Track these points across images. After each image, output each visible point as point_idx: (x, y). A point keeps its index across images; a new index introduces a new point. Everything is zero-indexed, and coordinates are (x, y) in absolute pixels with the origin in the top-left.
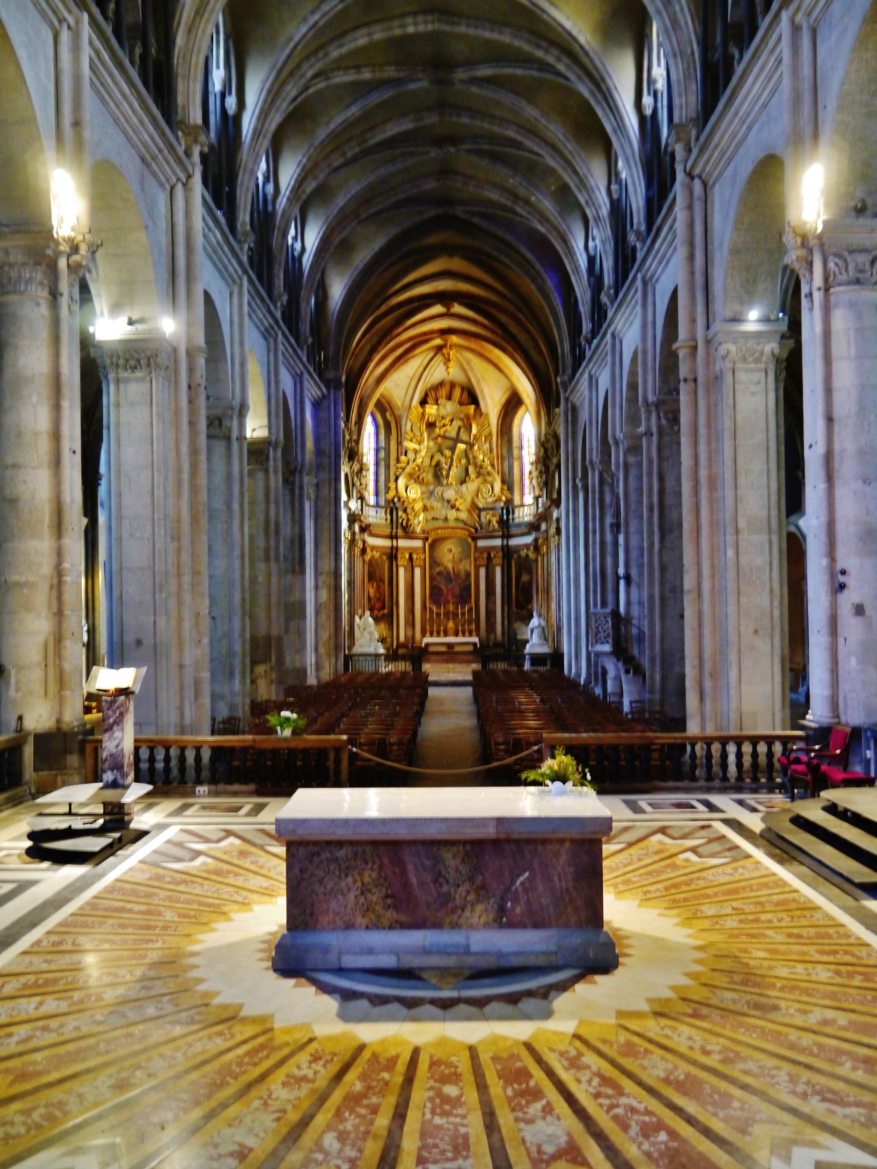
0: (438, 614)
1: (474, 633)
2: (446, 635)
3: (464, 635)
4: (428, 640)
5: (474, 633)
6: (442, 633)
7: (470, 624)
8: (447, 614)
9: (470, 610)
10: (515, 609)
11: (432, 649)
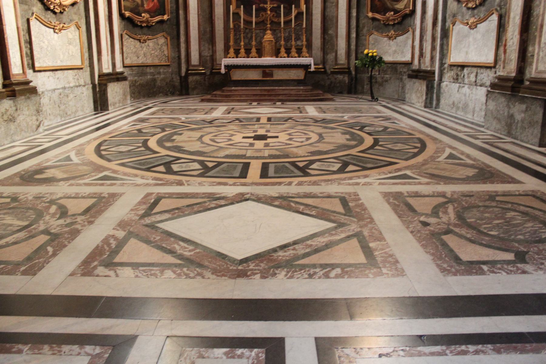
0: (248, 23)
1: (304, 49)
2: (260, 54)
3: (288, 53)
4: (225, 61)
5: (304, 49)
6: (254, 50)
7: (298, 38)
8: (261, 24)
9: (299, 15)
10: (370, 15)
11: (237, 75)
